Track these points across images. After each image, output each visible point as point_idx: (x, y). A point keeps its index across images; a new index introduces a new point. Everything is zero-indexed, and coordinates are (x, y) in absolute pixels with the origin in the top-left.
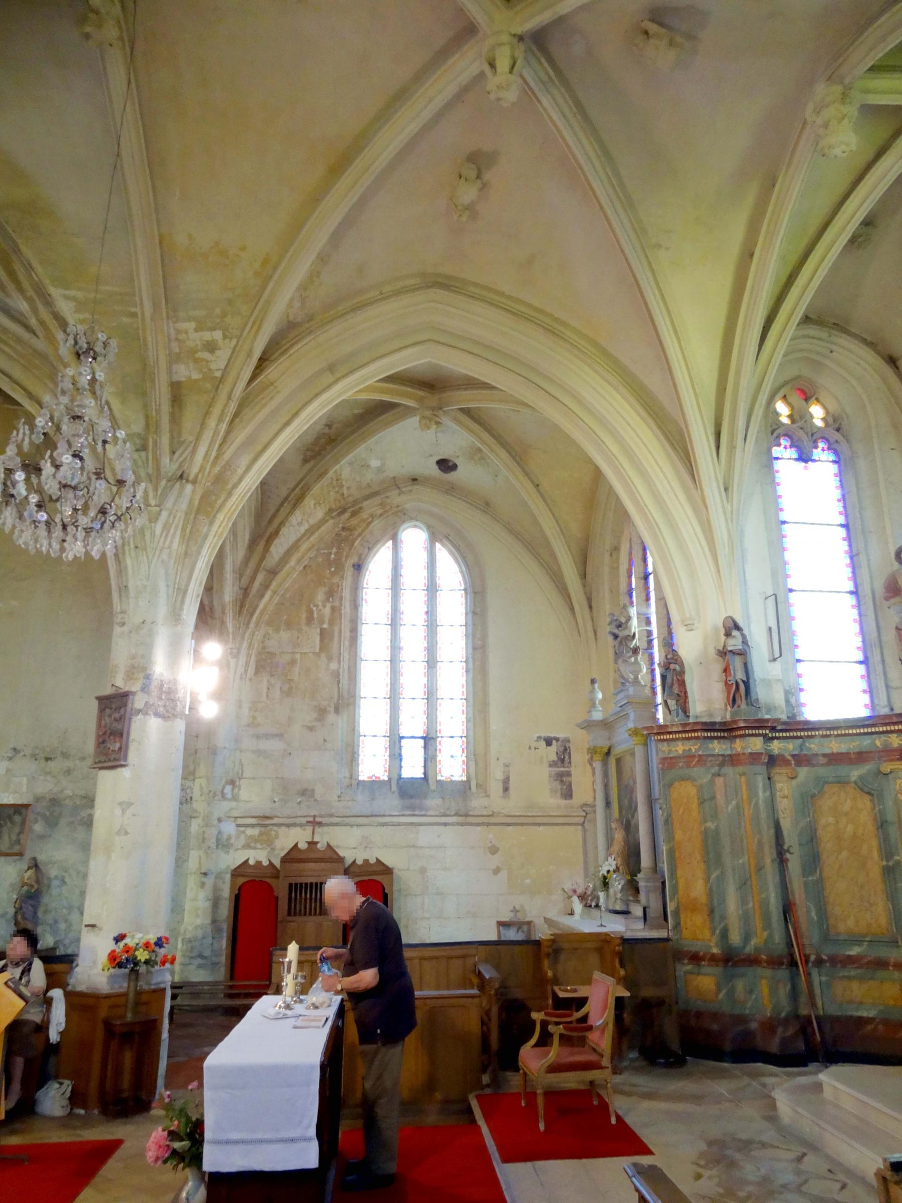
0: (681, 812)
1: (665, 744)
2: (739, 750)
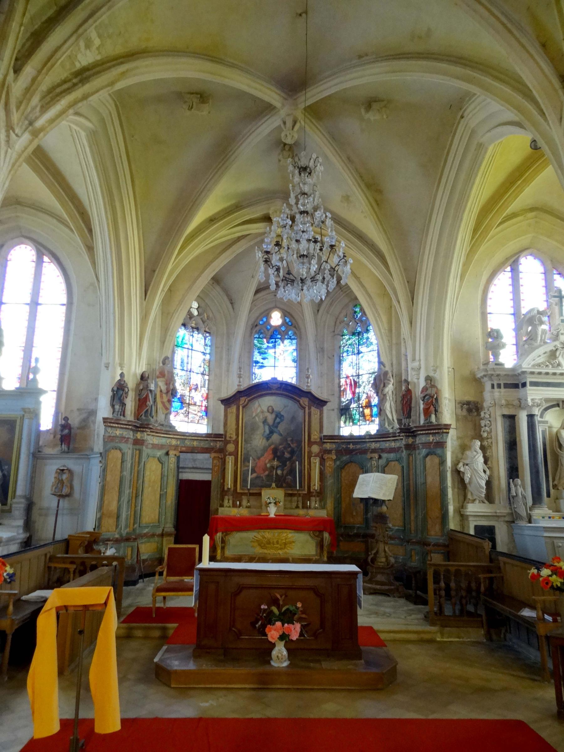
0: (112, 465)
1: (110, 429)
2: (139, 437)
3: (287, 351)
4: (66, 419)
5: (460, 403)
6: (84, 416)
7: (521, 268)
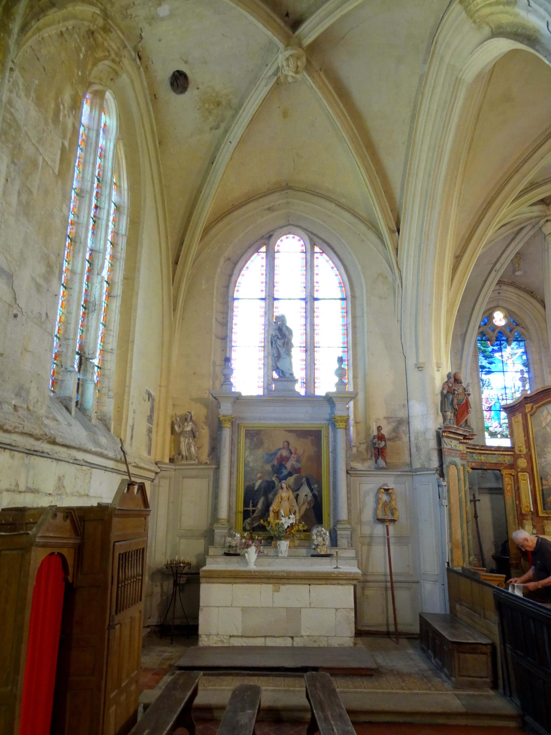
3: (516, 354)
4: (379, 428)
6: (394, 424)
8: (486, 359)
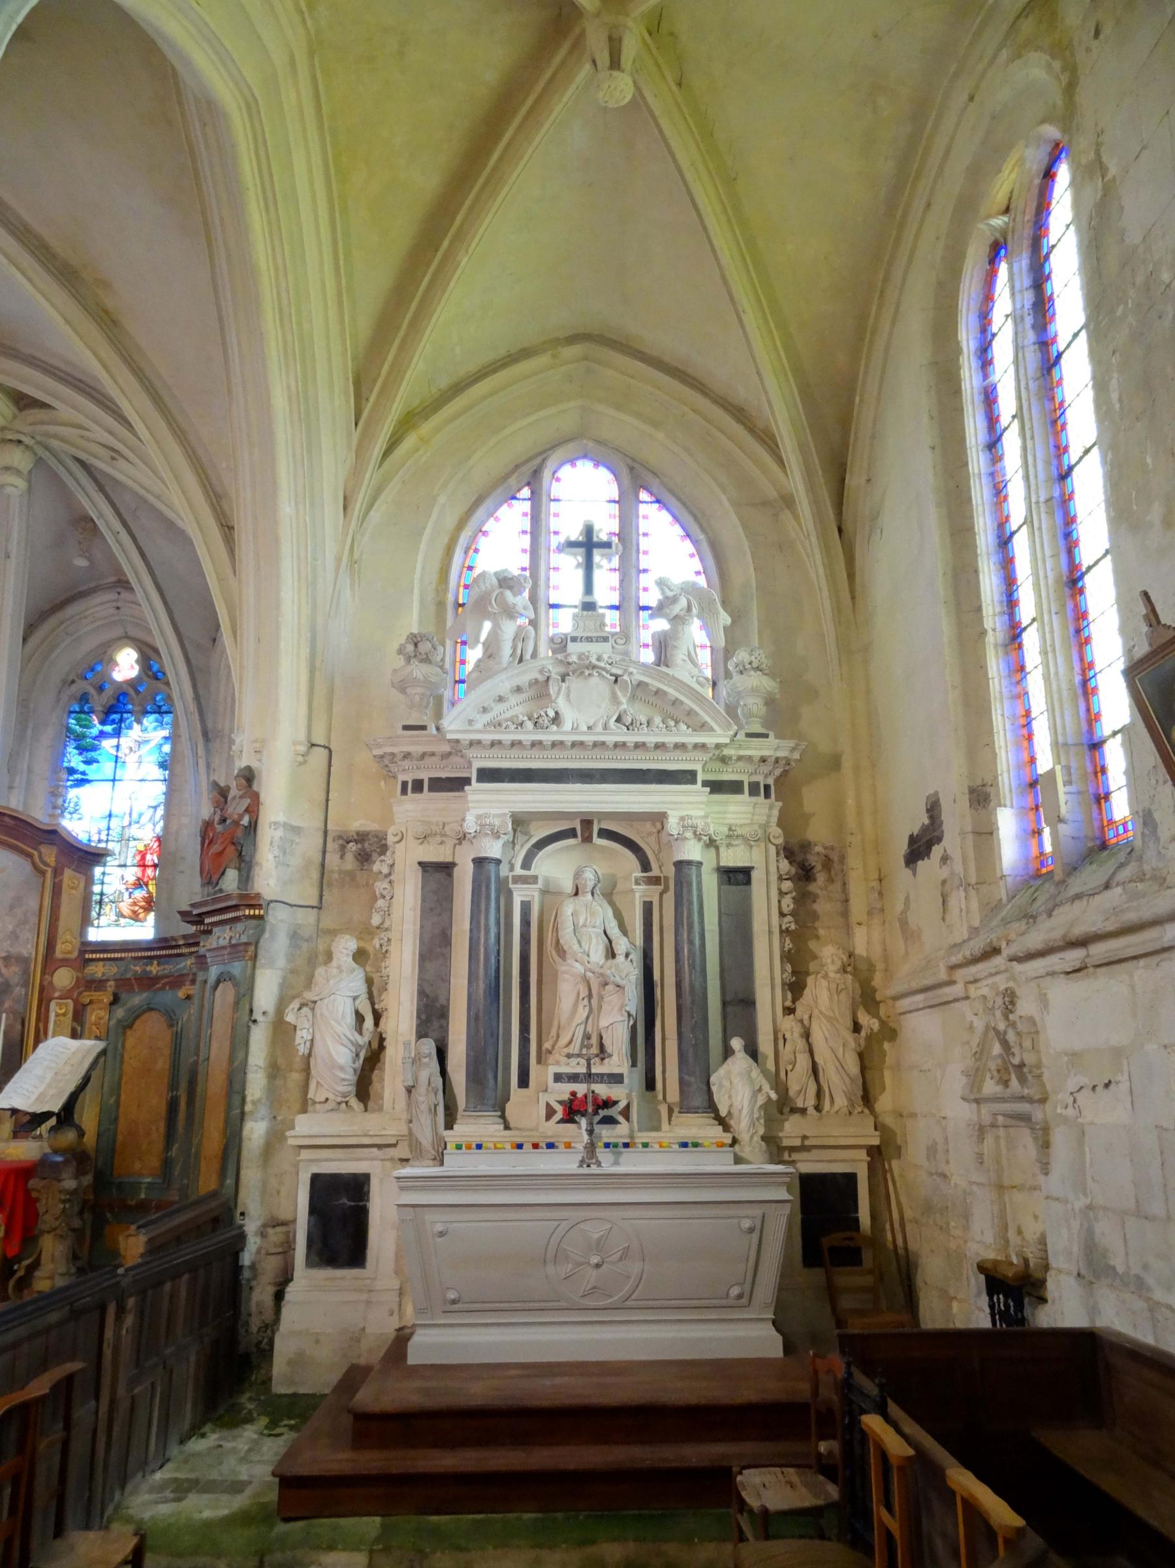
3: (148, 741)
5: (340, 837)
7: (556, 490)
8: (80, 754)
